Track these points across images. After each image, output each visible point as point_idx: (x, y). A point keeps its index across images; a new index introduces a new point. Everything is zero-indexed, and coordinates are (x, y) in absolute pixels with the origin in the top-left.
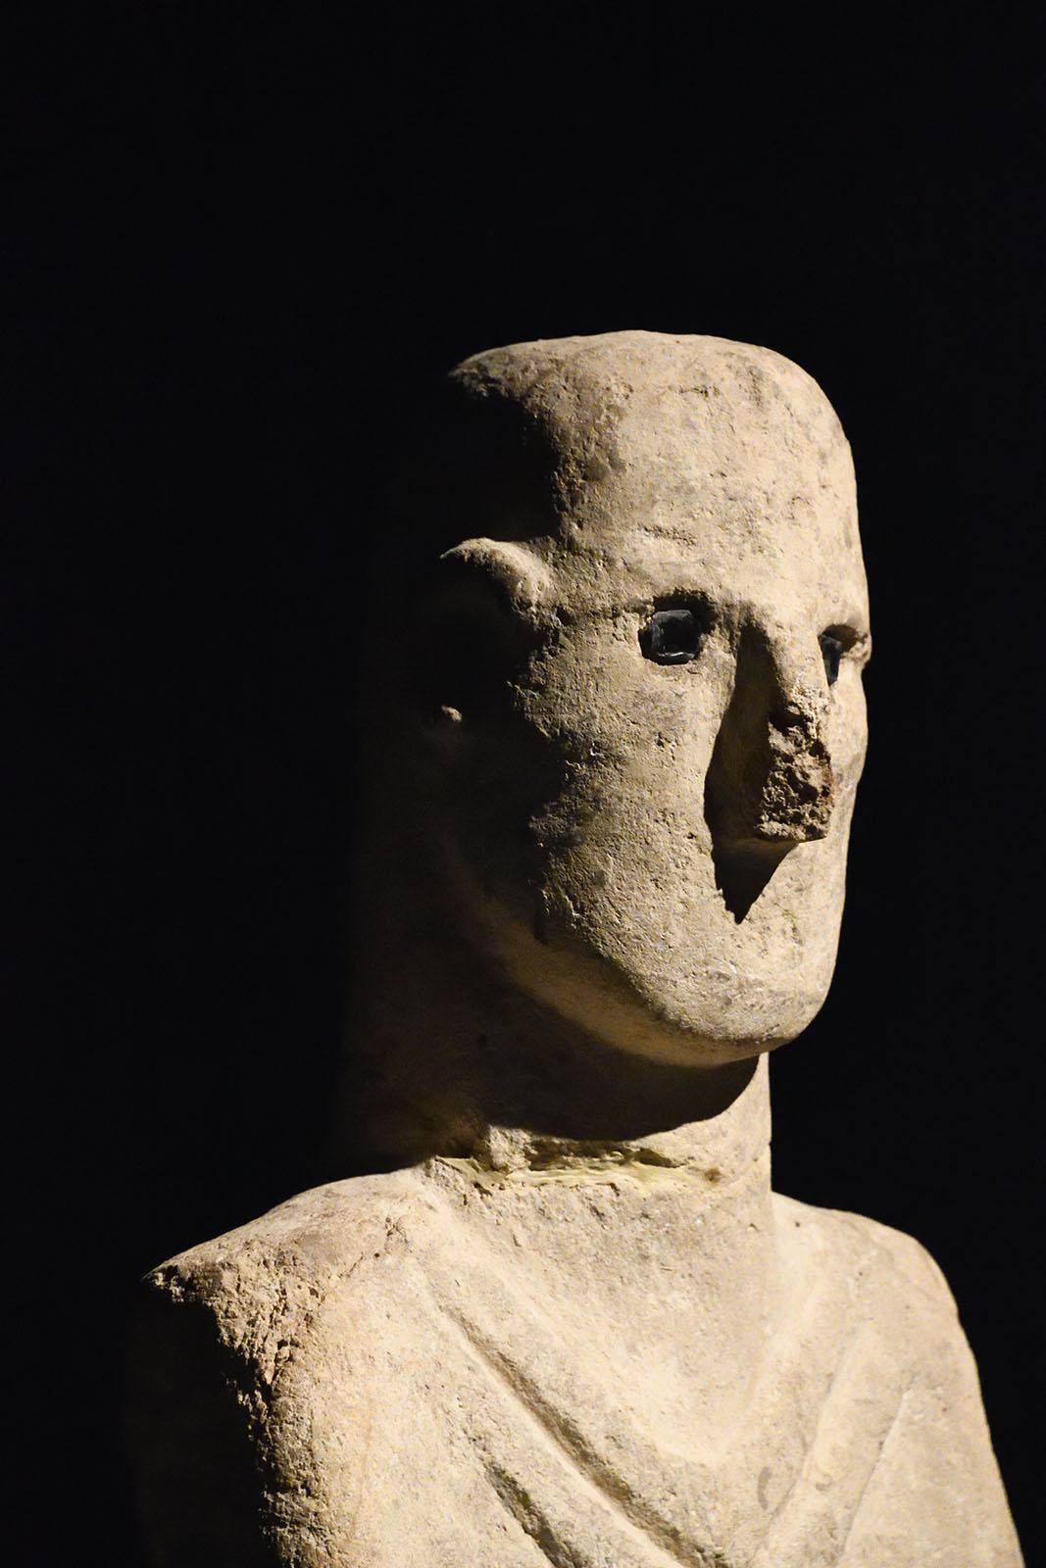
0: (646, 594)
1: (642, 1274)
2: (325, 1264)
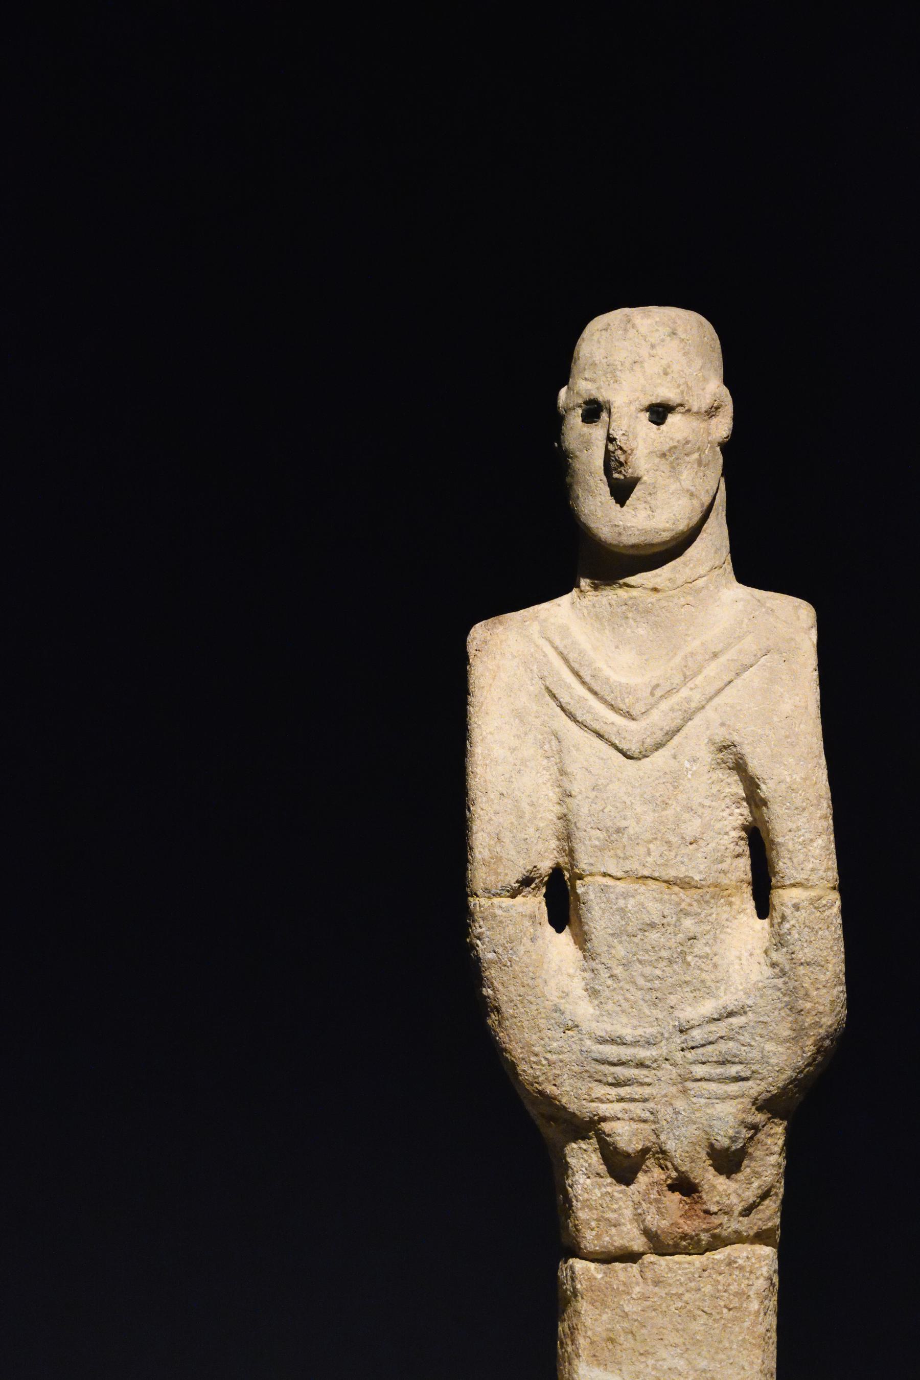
0: (580, 401)
1: (626, 623)
2: (498, 625)
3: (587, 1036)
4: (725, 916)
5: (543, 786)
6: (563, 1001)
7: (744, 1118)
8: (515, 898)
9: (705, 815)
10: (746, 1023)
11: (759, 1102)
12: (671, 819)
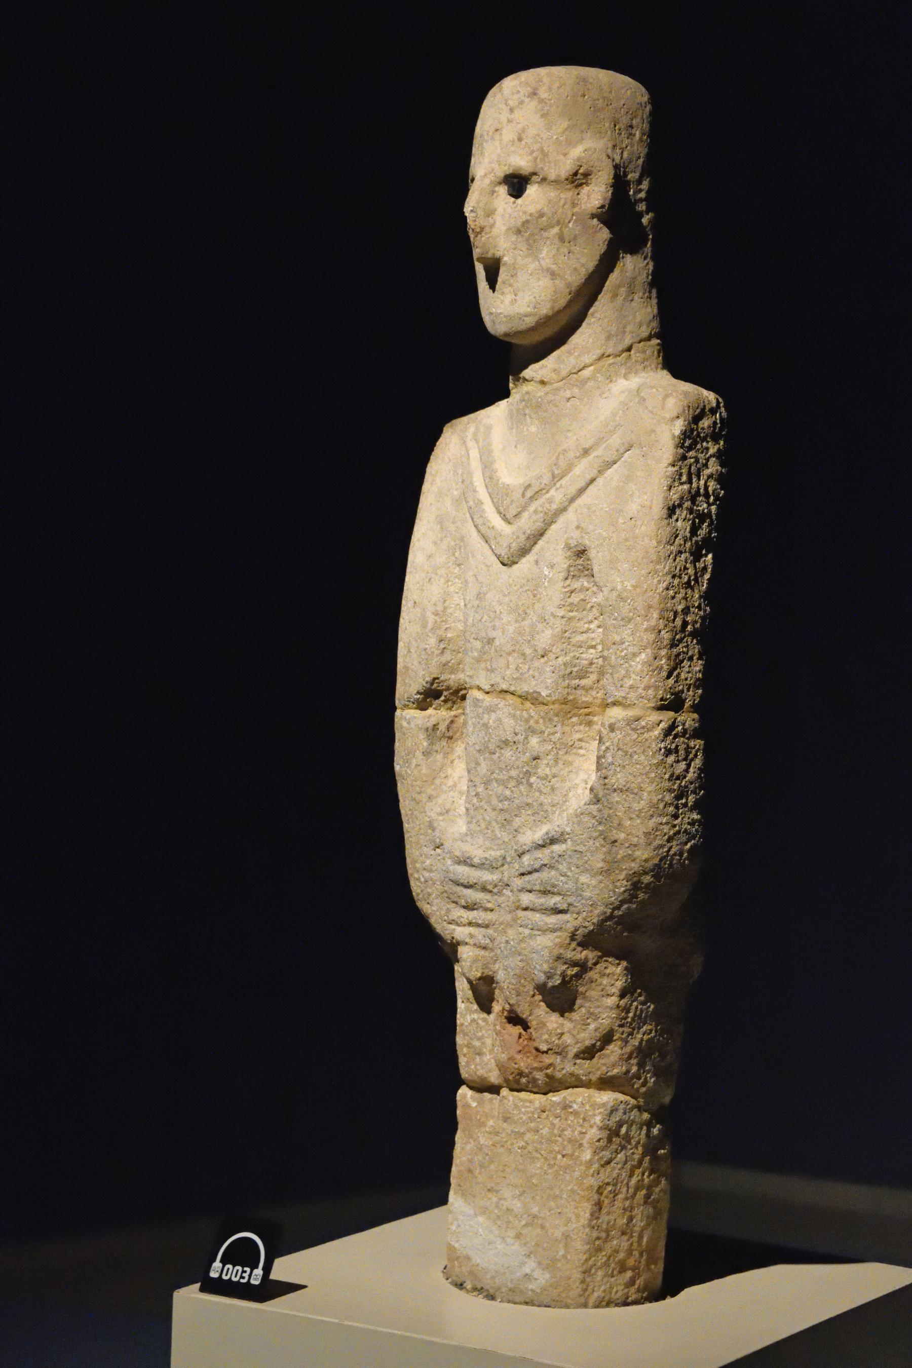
3: (448, 855)
4: (577, 736)
5: (456, 595)
6: (441, 818)
7: (561, 954)
8: (425, 709)
9: (556, 626)
10: (564, 851)
11: (579, 938)
12: (528, 630)
